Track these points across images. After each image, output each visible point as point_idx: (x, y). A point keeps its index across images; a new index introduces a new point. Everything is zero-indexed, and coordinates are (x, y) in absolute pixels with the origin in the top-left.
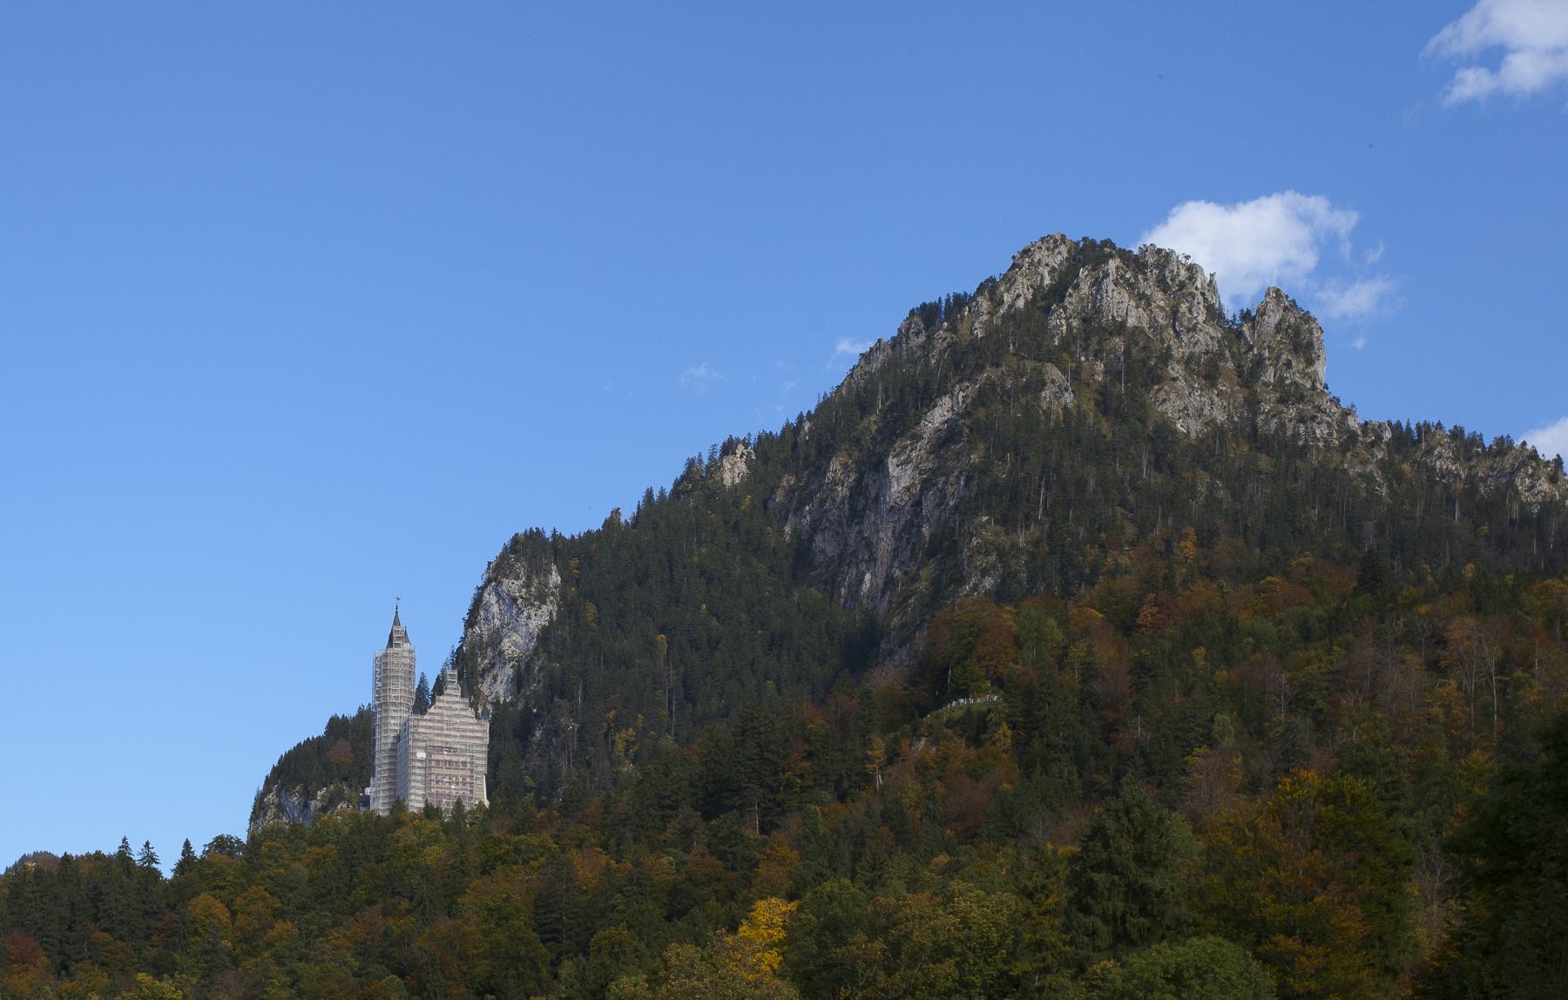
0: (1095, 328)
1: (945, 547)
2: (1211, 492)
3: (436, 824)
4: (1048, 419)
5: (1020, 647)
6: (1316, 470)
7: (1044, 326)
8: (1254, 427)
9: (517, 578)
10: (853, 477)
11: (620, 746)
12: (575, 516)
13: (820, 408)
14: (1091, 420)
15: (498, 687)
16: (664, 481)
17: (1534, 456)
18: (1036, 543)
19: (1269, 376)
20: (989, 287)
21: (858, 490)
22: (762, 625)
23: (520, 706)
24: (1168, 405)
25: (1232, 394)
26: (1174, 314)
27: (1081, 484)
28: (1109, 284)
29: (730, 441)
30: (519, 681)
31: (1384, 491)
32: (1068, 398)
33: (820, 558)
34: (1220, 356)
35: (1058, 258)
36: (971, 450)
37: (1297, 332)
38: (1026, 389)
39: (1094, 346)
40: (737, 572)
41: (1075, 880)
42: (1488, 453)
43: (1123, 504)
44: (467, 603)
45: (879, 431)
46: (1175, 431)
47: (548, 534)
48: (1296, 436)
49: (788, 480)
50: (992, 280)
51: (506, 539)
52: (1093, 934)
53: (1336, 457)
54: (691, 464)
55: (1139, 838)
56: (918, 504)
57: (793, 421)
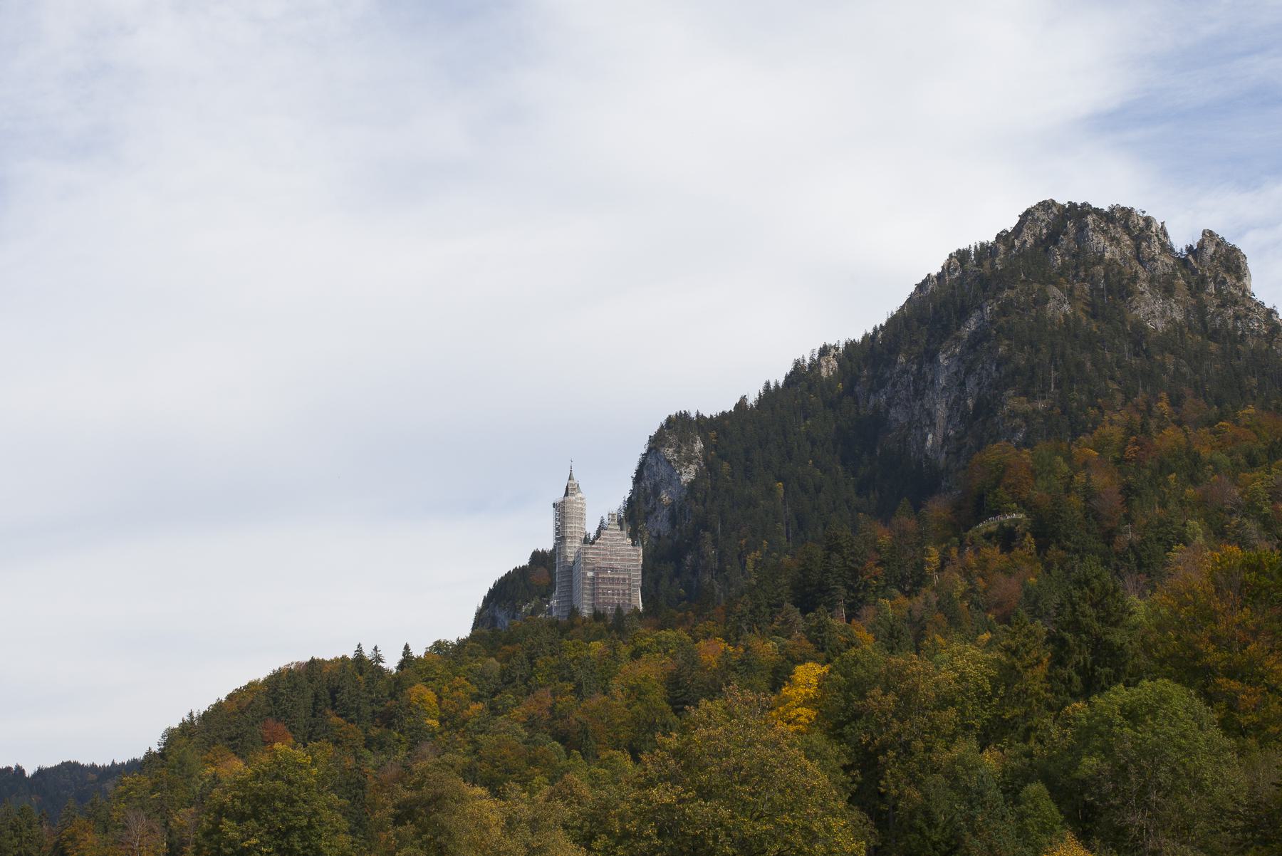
2: (1177, 369)
6: (1252, 351)
14: (1084, 322)
15: (661, 524)
16: (778, 376)
19: (1211, 288)
27: (1080, 366)
32: (1066, 307)
37: (1227, 259)
38: (1036, 302)
43: (1112, 378)
46: (1146, 328)
47: (693, 415)
48: (1235, 328)
51: (662, 419)
54: (797, 363)
57: (870, 331)
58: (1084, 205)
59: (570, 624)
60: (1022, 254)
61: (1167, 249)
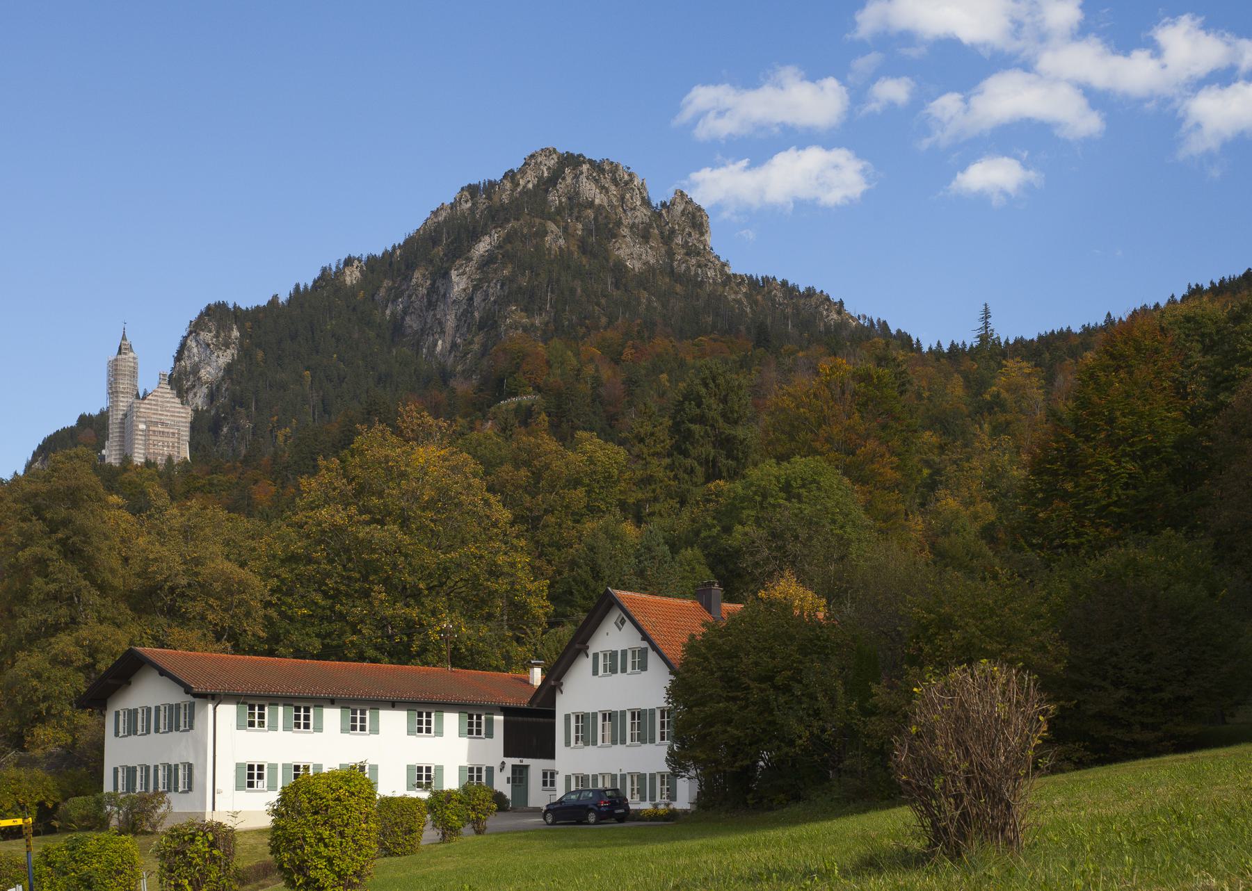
0: (575, 203)
1: (489, 324)
3: (153, 471)
4: (550, 254)
5: (550, 367)
7: (545, 201)
8: (672, 266)
9: (210, 331)
10: (429, 282)
11: (281, 438)
12: (250, 295)
13: (406, 242)
16: (307, 278)
17: (827, 299)
18: (547, 324)
19: (679, 240)
20: (510, 175)
21: (433, 289)
22: (373, 368)
23: (213, 412)
24: (621, 251)
25: (658, 248)
26: (622, 199)
28: (583, 178)
29: (350, 257)
30: (212, 397)
31: (748, 310)
32: (562, 242)
33: (409, 331)
34: (650, 226)
35: (552, 162)
36: (505, 267)
37: (694, 217)
38: (536, 234)
39: (575, 214)
40: (356, 336)
41: (676, 428)
42: (802, 296)
44: (176, 346)
45: (445, 255)
47: (231, 306)
48: (697, 275)
49: (387, 283)
50: (512, 171)
51: (203, 307)
52: (691, 472)
53: (720, 289)
54: (324, 270)
55: (724, 400)
56: (471, 299)
57: (390, 249)
58: (580, 155)
59: (113, 478)
60: (525, 192)
61: (646, 202)
